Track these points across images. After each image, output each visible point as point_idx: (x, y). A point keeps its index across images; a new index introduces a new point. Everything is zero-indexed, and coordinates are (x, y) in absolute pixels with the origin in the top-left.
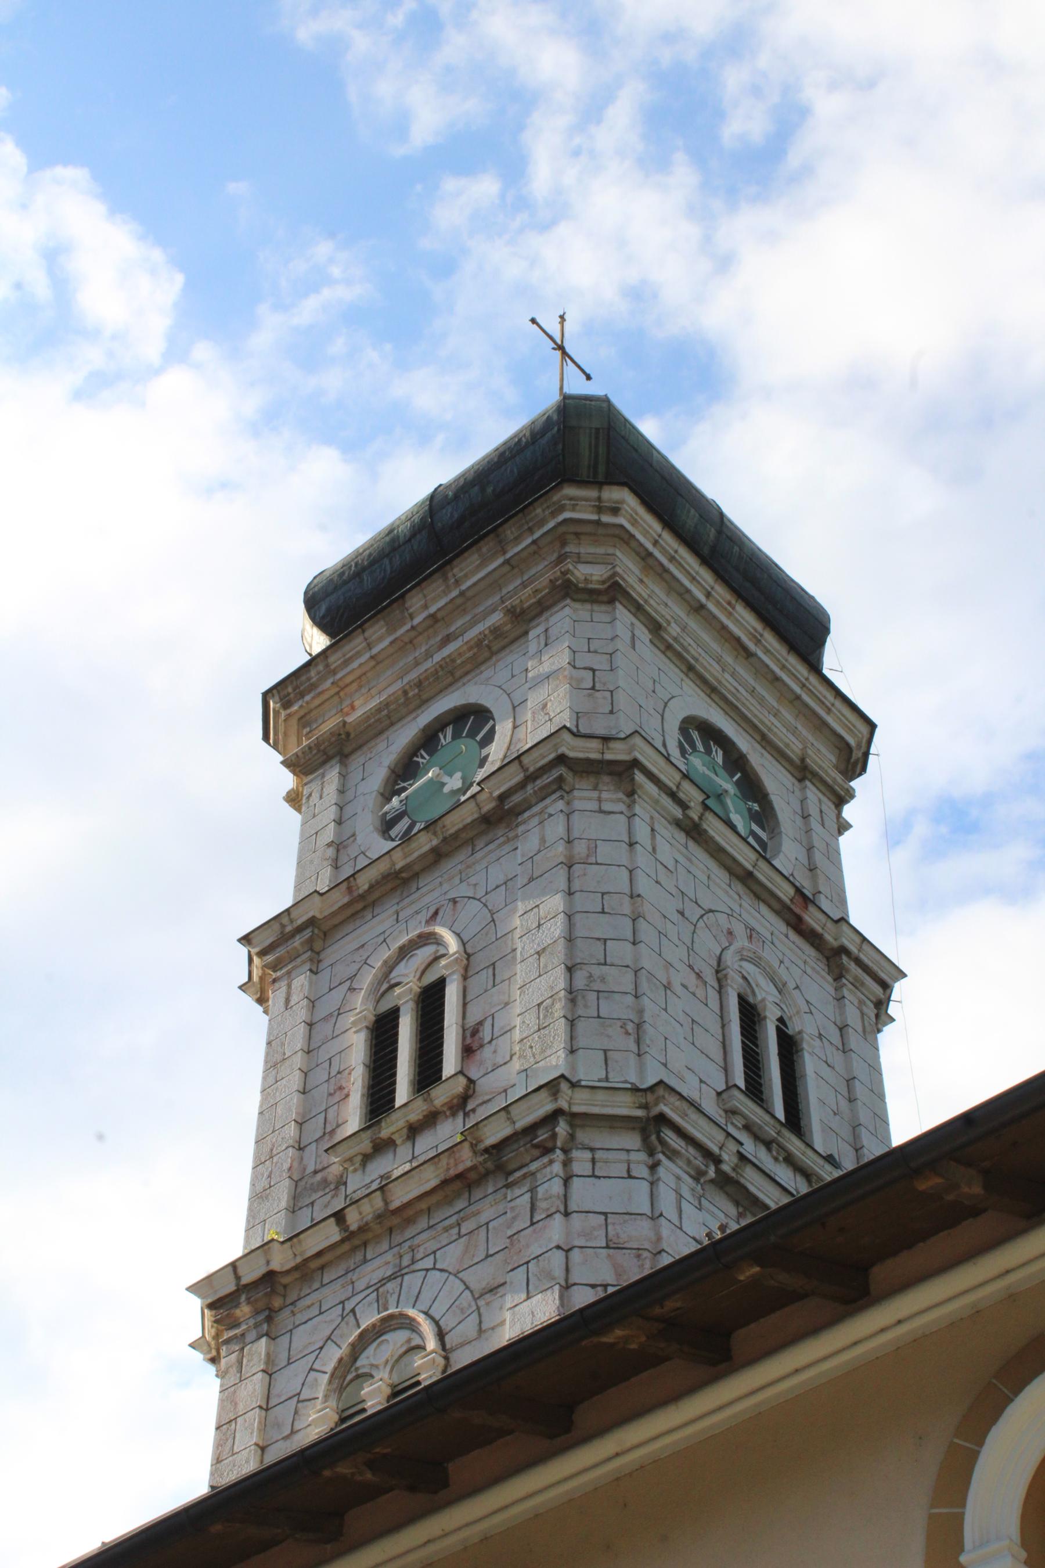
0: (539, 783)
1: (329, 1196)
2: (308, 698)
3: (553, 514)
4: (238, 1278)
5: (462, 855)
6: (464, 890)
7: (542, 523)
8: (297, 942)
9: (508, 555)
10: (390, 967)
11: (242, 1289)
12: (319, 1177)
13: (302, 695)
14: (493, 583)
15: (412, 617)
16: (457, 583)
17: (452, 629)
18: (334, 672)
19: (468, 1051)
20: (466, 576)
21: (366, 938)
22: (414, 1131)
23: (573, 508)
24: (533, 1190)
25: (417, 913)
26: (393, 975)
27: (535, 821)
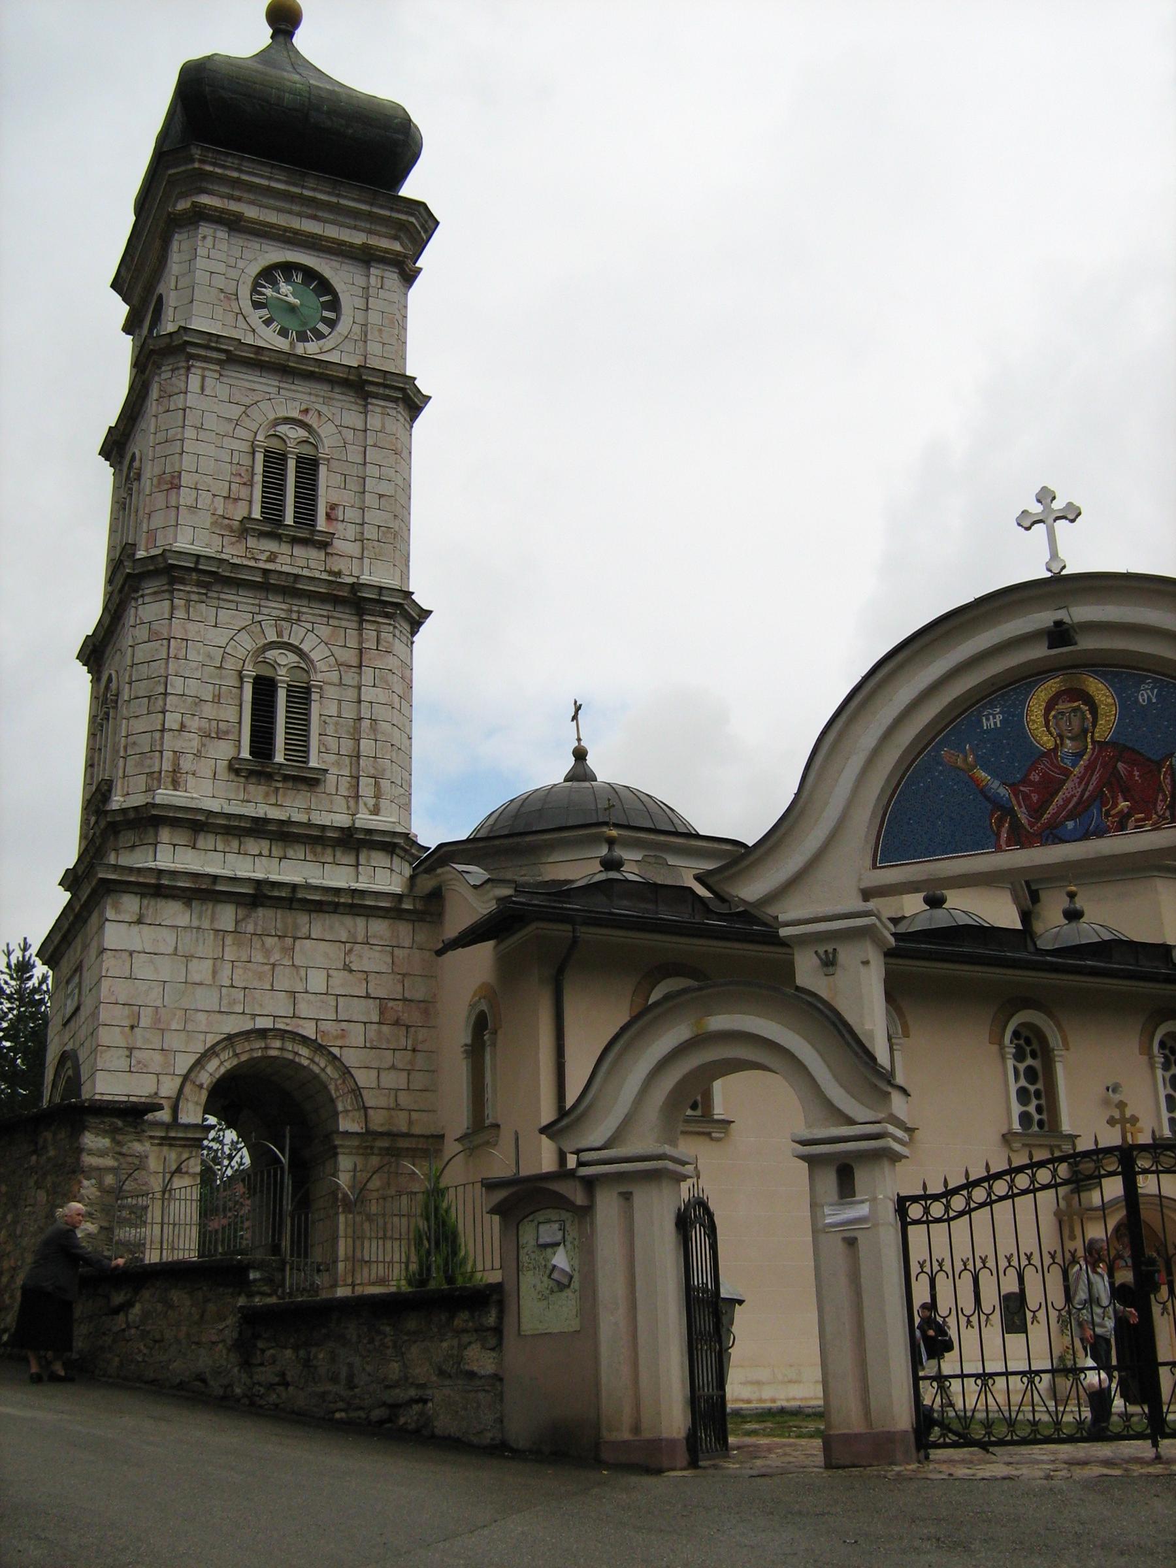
0: (387, 392)
1: (234, 539)
2: (219, 171)
3: (407, 213)
4: (197, 563)
5: (326, 387)
6: (324, 409)
7: (398, 211)
8: (215, 355)
9: (375, 210)
10: (277, 422)
11: (196, 570)
12: (227, 521)
13: (214, 164)
14: (355, 214)
15: (303, 187)
16: (338, 196)
17: (320, 214)
18: (240, 171)
19: (328, 515)
20: (345, 197)
21: (256, 387)
22: (295, 541)
23: (417, 219)
24: (378, 632)
25: (294, 399)
26: (279, 428)
27: (378, 410)
